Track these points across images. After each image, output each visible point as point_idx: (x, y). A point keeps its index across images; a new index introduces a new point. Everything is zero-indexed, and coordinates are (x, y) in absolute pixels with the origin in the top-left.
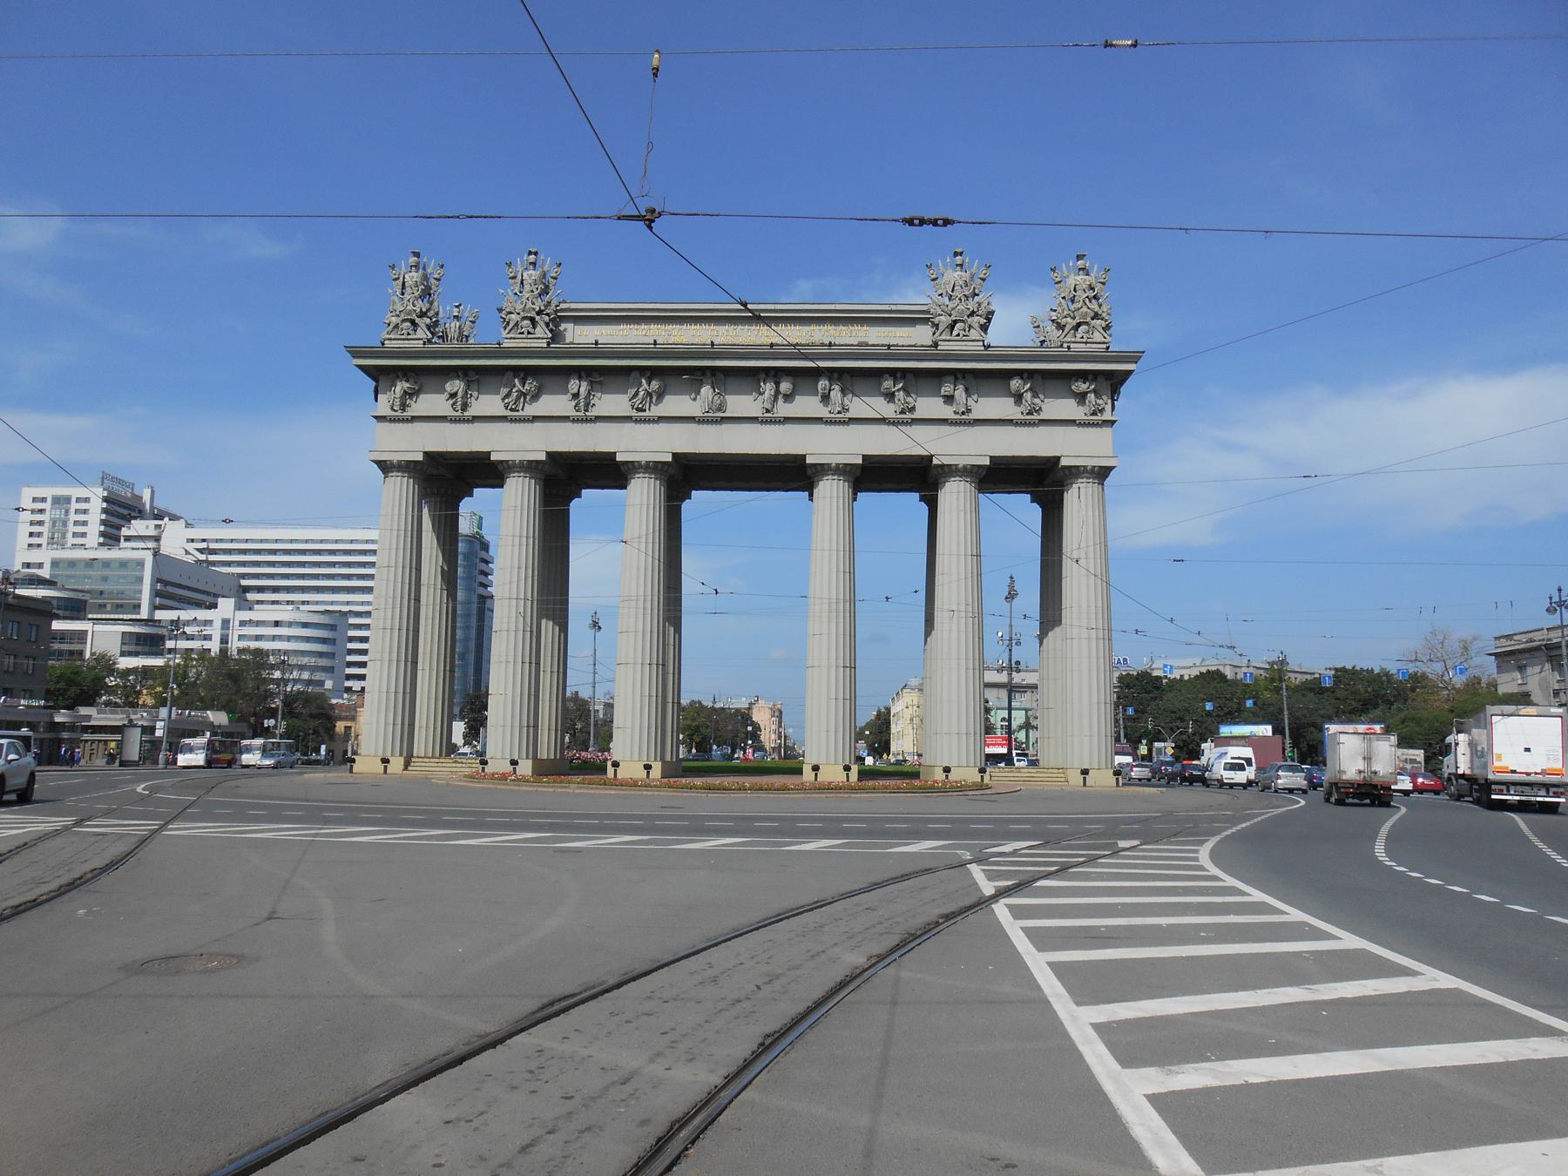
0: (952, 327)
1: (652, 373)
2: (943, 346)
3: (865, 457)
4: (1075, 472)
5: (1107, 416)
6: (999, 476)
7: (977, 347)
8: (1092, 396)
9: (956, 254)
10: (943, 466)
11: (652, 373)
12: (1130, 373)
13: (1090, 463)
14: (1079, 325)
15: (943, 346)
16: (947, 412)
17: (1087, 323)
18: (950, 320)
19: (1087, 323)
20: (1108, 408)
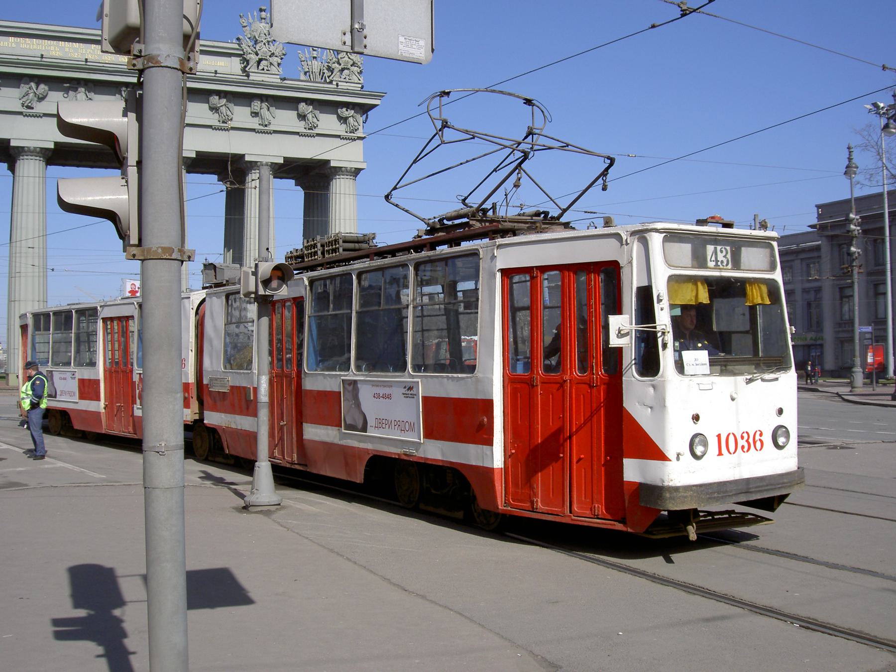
0: (259, 62)
1: (40, 80)
2: (253, 77)
3: (198, 153)
4: (338, 170)
5: (360, 134)
6: (291, 169)
7: (276, 80)
8: (351, 119)
9: (261, 10)
10: (251, 162)
11: (40, 80)
12: (375, 106)
13: (349, 165)
14: (342, 70)
15: (253, 77)
16: (254, 123)
17: (348, 69)
18: (257, 58)
19: (348, 69)
20: (361, 128)
